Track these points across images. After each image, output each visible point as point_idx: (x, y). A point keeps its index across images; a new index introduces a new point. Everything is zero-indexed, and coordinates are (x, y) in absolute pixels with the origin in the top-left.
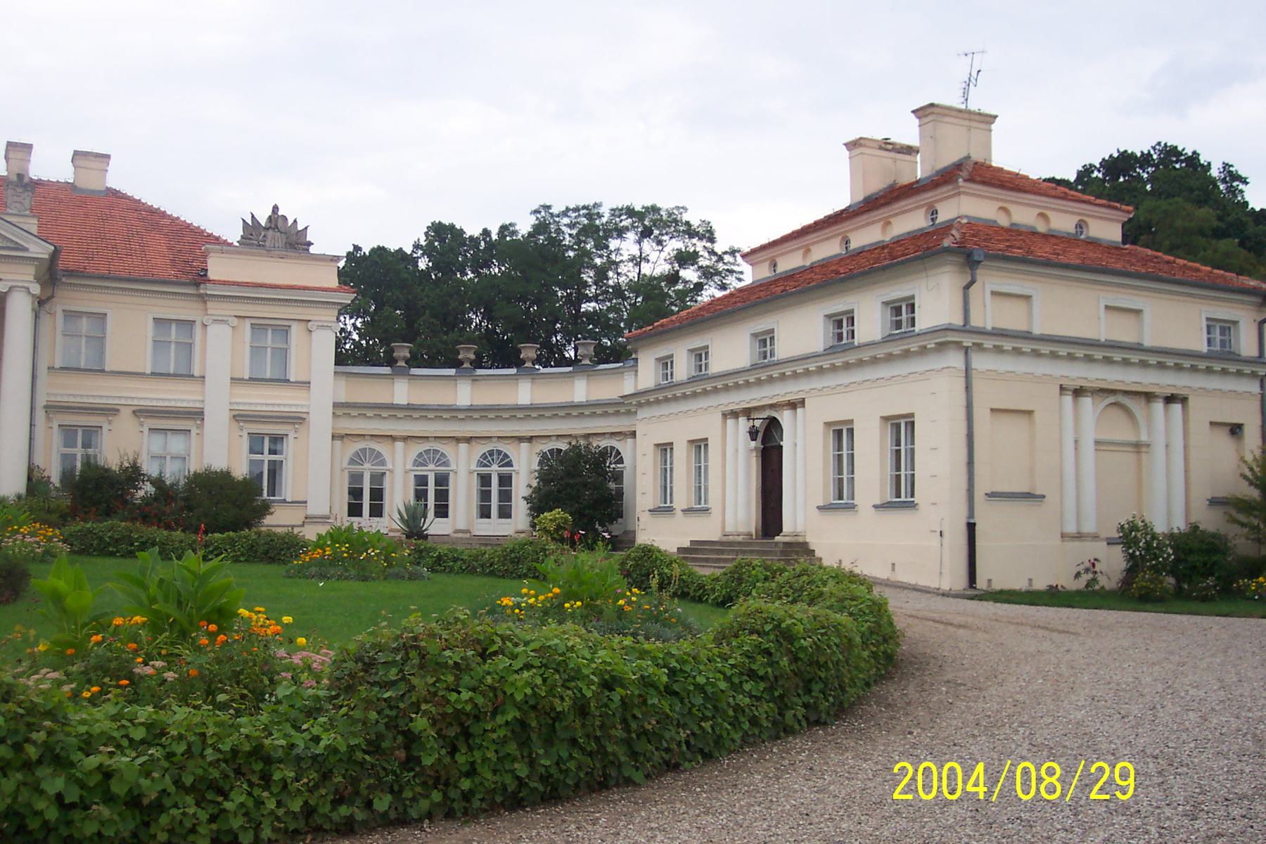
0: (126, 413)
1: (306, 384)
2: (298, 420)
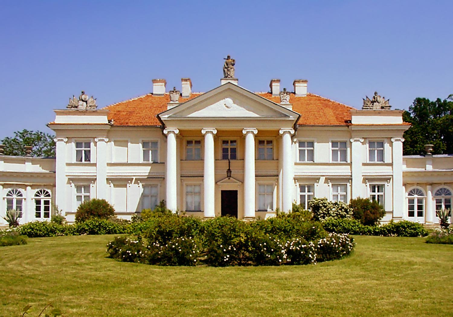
0: (323, 179)
1: (391, 165)
2: (388, 179)
